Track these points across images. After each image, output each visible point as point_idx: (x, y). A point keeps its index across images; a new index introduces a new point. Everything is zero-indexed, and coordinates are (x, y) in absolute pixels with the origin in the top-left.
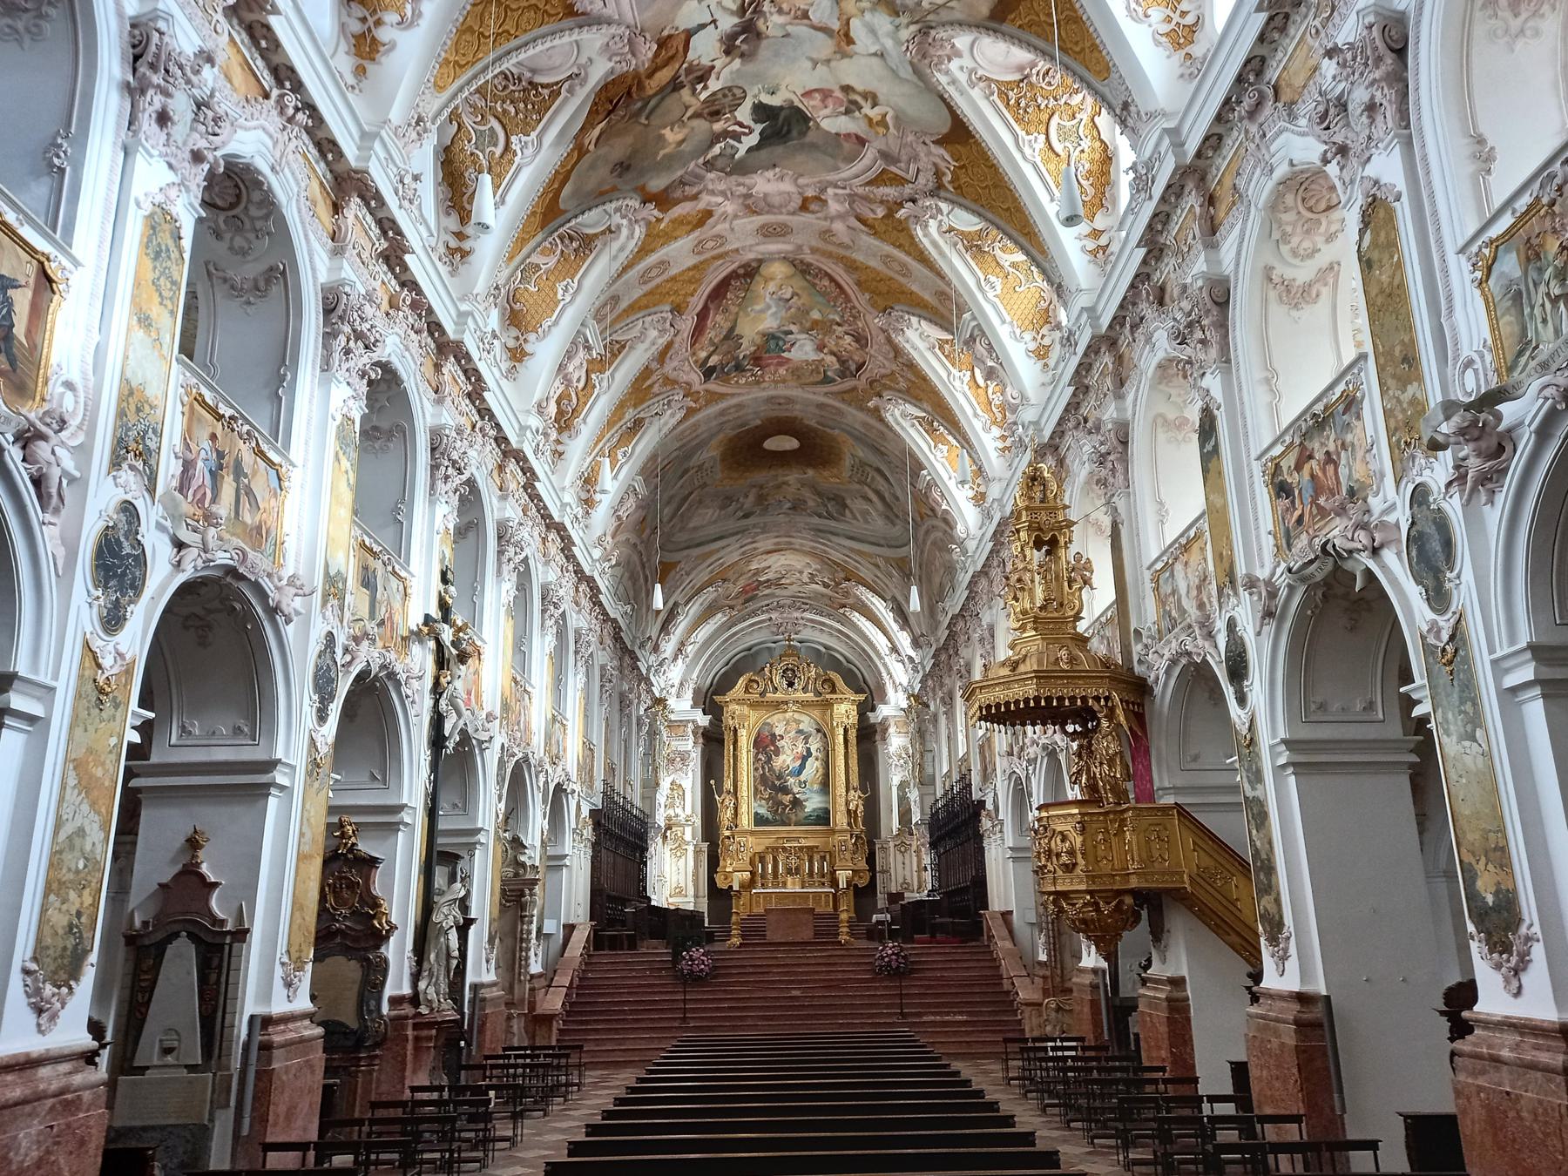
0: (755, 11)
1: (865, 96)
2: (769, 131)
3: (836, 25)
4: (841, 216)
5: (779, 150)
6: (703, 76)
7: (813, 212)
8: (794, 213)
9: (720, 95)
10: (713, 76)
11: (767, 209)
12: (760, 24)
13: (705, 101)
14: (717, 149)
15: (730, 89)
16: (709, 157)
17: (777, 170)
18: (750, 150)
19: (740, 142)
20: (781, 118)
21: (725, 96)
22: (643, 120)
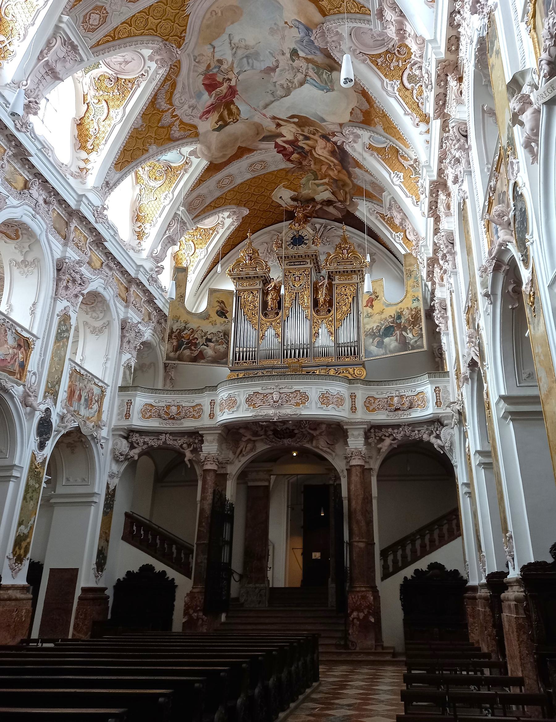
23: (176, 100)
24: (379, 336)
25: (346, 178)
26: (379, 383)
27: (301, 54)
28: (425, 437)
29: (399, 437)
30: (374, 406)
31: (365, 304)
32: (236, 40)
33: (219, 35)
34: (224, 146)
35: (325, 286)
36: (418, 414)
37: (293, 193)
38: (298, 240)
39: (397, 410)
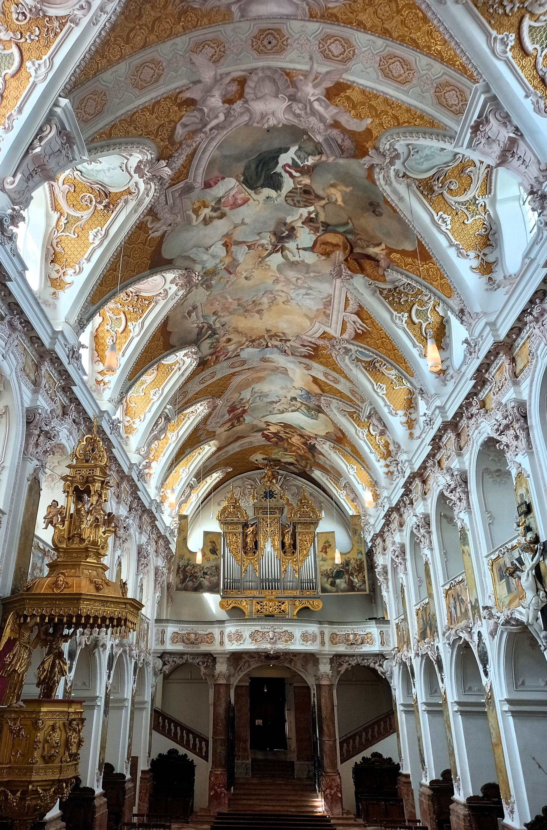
0: (276, 246)
1: (211, 219)
2: (271, 165)
3: (234, 248)
4: (208, 92)
5: (265, 147)
6: (309, 221)
7: (233, 80)
8: (252, 71)
9: (302, 204)
10: (304, 218)
11: (276, 76)
12: (274, 239)
13: (312, 204)
14: (310, 161)
15: (295, 205)
16: (317, 158)
17: (266, 126)
18: (286, 150)
19: (293, 159)
20: (263, 177)
21: (299, 202)
22: (350, 226)
23: (208, 423)
24: (332, 577)
25: (311, 458)
26: (339, 623)
27: (298, 400)
28: (372, 665)
29: (353, 663)
30: (337, 640)
31: (320, 549)
32: (256, 390)
33: (246, 389)
34: (228, 437)
35: (290, 533)
36: (366, 649)
37: (264, 456)
38: (270, 494)
39: (352, 644)
